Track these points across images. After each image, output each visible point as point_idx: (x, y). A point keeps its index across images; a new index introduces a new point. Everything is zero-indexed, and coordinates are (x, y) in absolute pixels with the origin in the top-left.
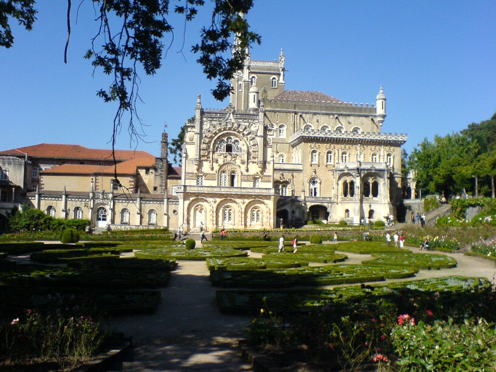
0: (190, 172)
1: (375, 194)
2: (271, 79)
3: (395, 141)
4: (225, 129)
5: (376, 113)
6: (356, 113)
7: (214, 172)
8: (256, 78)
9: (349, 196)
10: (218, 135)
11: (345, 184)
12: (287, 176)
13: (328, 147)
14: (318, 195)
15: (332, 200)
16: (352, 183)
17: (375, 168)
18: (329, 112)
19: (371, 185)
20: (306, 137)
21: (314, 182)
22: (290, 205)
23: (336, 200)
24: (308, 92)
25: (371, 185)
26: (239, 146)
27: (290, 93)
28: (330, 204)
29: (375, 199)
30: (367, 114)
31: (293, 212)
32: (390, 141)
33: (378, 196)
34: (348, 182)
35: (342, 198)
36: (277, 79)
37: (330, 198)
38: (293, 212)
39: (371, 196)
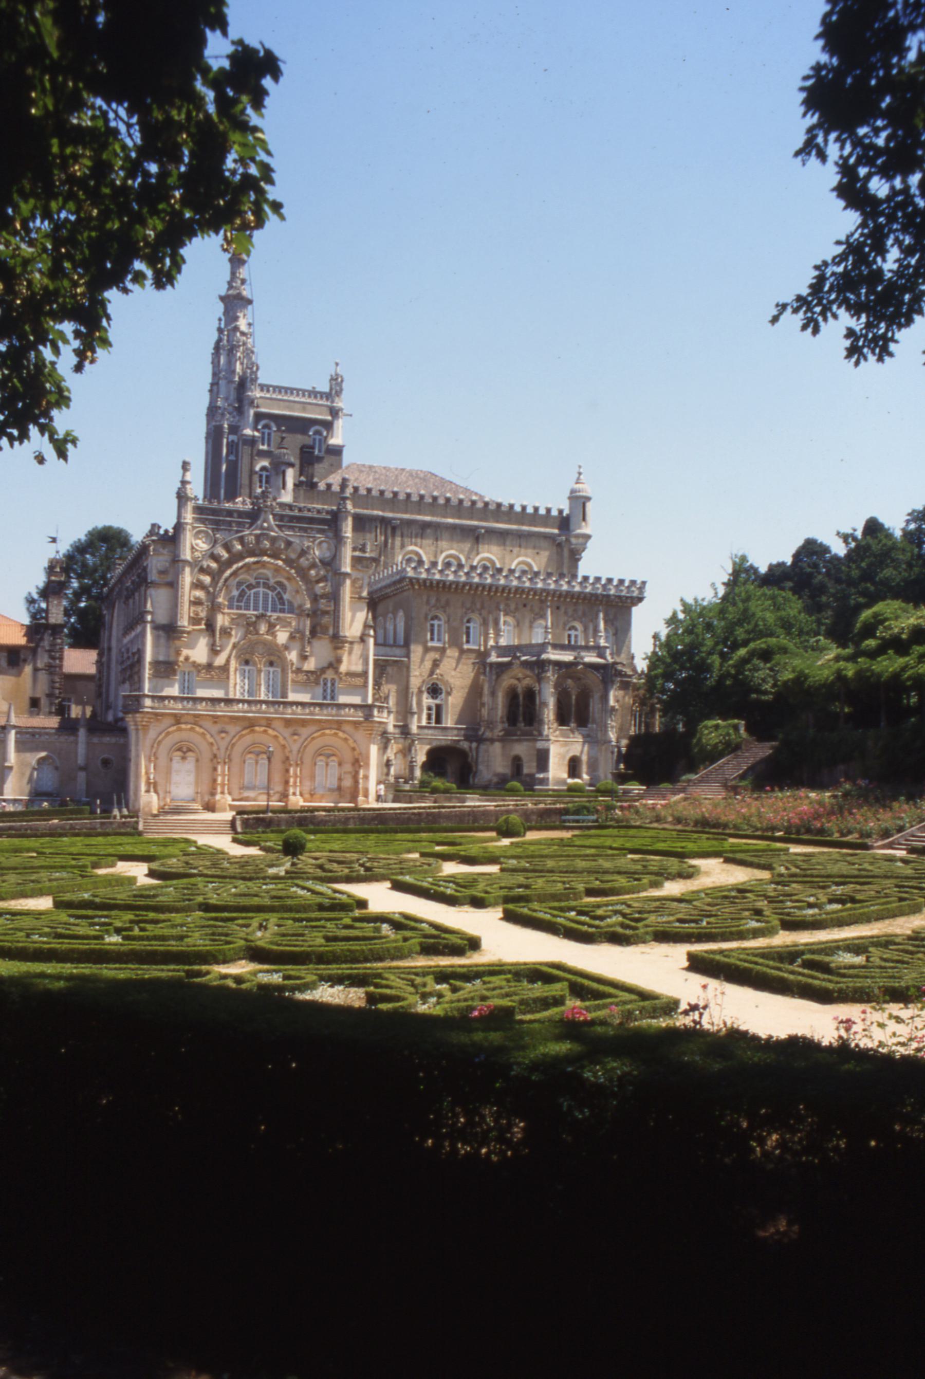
0: (161, 658)
4: (252, 554)
7: (220, 661)
9: (521, 725)
10: (235, 567)
11: (512, 695)
15: (480, 733)
16: (531, 695)
23: (488, 734)
24: (403, 470)
26: (286, 597)
27: (361, 471)
28: (474, 745)
34: (520, 690)
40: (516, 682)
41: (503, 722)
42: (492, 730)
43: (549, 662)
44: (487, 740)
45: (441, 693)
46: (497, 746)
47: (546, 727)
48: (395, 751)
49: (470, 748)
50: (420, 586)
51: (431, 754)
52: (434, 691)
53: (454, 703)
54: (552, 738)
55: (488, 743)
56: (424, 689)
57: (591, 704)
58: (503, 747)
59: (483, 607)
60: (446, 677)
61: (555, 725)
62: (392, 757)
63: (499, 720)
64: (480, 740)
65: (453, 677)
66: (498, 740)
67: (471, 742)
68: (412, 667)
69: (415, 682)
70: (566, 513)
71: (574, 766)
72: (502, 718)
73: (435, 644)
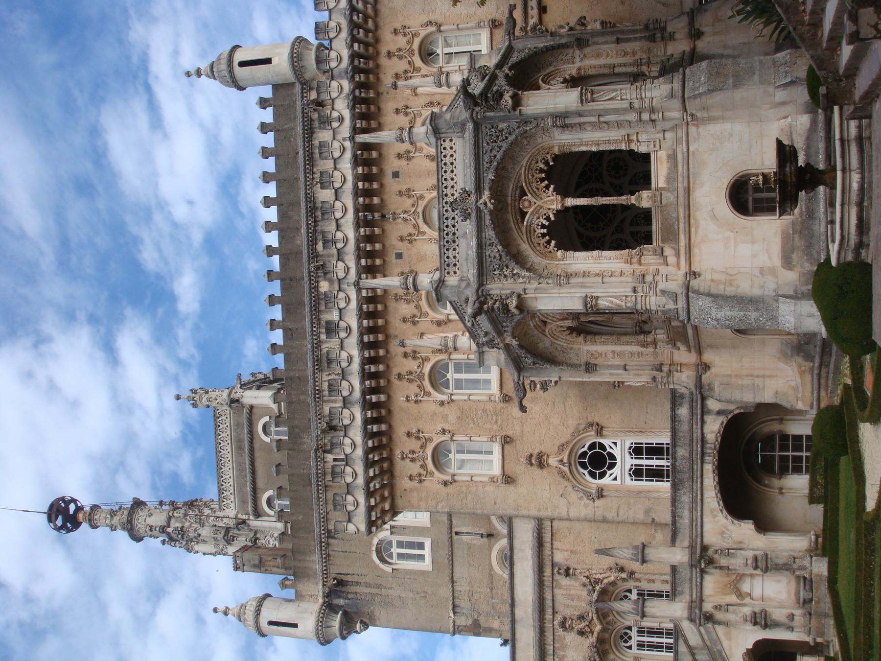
1: (632, 169)
2: (267, 440)
3: (353, 26)
5: (292, 85)
6: (302, 177)
8: (270, 493)
12: (572, 598)
13: (413, 389)
14: (665, 439)
17: (466, 193)
18: (306, 300)
19: (570, 202)
20: (370, 509)
21: (598, 461)
22: (720, 630)
25: (570, 202)
29: (660, 172)
30: (299, 130)
31: (761, 619)
32: (353, 56)
33: (643, 149)
36: (267, 419)
37: (675, 399)
38: (761, 619)
39: (644, 199)
44: (699, 379)
45: (602, 447)
48: (733, 599)
49: (719, 413)
50: (383, 499)
52: (598, 461)
55: (705, 378)
57: (584, 148)
58: (711, 346)
59: (414, 355)
64: (702, 392)
66: (700, 352)
67: (704, 411)
70: (267, 92)
72: (644, 345)
73: (496, 457)
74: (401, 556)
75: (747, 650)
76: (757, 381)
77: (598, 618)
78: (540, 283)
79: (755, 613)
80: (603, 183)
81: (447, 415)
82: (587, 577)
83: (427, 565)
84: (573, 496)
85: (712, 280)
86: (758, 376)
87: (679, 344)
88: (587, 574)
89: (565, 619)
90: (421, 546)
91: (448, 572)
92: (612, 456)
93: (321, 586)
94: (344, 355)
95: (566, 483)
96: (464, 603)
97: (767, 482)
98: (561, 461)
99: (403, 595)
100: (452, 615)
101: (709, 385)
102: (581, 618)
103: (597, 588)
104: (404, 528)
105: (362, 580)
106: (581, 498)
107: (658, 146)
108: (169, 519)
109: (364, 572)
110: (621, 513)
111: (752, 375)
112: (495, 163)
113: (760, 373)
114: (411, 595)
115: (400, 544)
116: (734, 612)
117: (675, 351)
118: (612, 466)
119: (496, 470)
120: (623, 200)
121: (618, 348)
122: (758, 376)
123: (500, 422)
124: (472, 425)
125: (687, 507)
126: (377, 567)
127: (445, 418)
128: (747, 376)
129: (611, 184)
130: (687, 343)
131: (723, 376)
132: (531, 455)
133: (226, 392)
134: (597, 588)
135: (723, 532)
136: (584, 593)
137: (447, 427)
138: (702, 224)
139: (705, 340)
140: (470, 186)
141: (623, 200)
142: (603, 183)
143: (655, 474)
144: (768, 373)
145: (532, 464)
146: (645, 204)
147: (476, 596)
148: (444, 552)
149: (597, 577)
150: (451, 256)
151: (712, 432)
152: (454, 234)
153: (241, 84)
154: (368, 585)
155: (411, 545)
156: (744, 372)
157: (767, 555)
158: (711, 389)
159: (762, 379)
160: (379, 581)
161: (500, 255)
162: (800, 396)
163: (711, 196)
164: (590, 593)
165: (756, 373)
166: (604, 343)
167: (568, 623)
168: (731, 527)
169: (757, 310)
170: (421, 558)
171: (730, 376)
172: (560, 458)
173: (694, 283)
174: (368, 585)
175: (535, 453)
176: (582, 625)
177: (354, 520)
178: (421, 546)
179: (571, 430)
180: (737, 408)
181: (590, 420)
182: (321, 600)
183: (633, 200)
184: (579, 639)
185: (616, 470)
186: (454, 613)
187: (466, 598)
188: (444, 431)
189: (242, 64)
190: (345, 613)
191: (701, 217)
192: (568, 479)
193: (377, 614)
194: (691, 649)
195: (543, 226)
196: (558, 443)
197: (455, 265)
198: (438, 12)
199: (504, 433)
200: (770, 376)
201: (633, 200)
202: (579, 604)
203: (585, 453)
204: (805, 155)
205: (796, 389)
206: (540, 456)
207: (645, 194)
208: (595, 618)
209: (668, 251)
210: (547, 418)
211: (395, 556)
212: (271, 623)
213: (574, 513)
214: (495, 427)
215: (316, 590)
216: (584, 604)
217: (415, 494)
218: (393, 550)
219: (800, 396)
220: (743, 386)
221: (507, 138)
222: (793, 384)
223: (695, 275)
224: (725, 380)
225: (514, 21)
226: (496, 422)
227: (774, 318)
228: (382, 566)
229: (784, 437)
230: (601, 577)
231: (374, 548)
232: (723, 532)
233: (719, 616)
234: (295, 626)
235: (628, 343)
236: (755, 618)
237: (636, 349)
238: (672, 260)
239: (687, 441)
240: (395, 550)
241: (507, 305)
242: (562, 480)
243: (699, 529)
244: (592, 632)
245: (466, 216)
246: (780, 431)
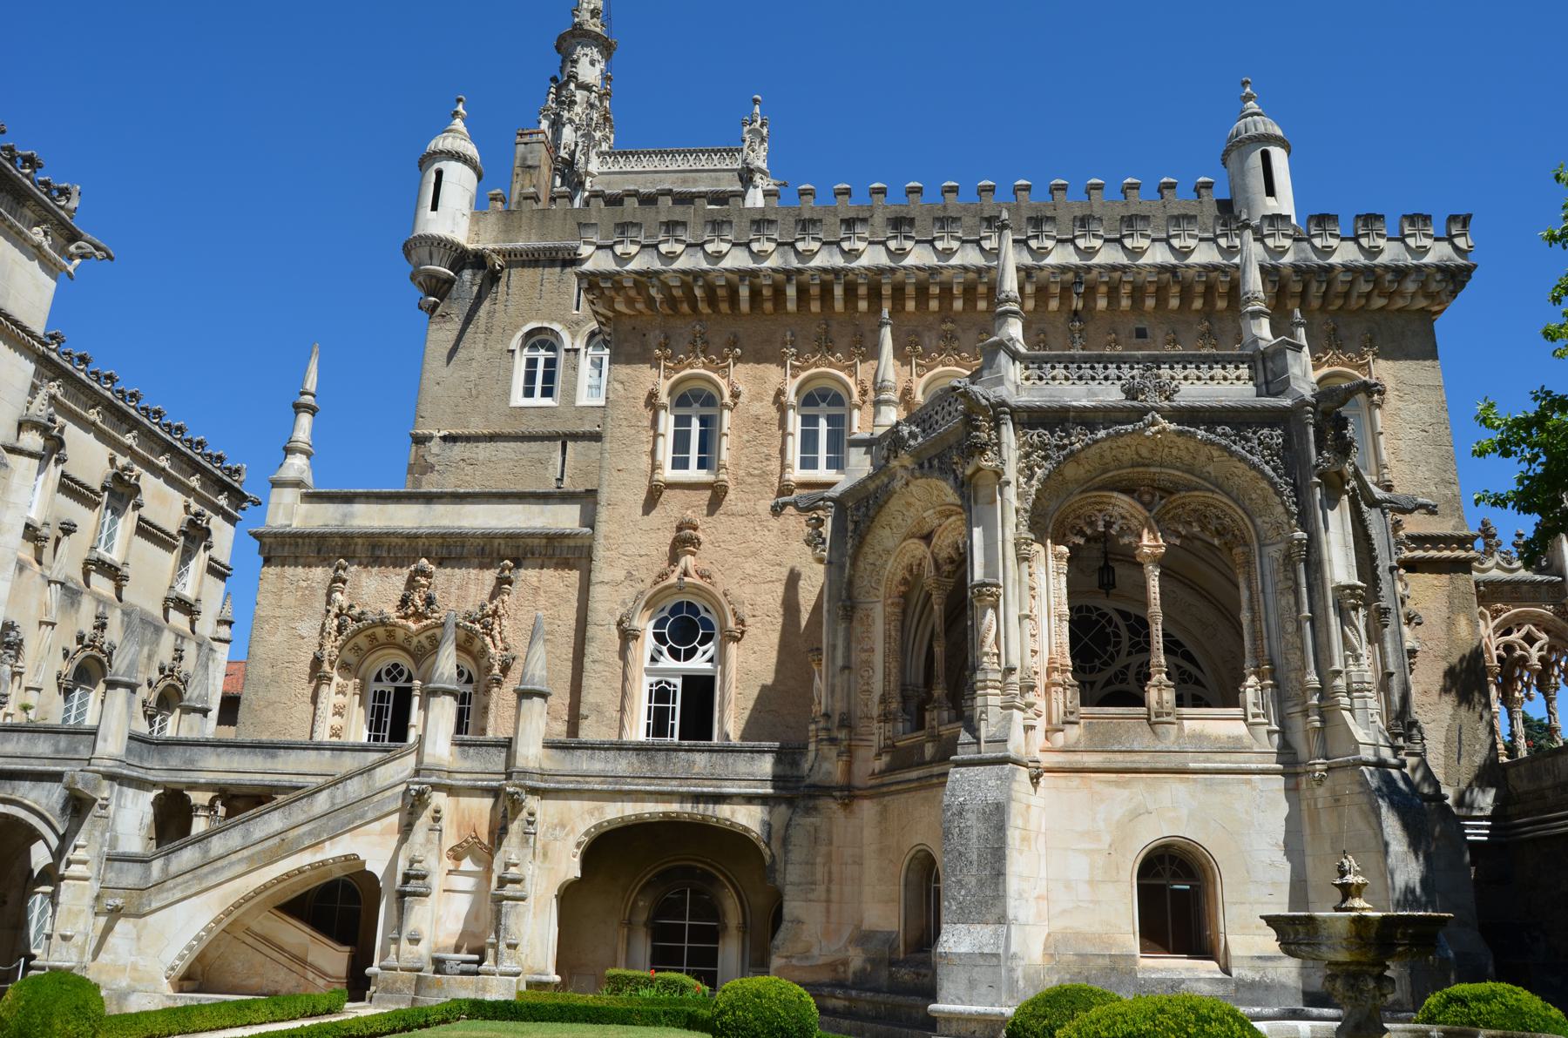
35: (889, 748)
39: (1159, 693)
40: (917, 548)
41: (886, 717)
42: (849, 753)
43: (998, 412)
44: (824, 790)
46: (867, 809)
47: (995, 700)
48: (450, 840)
50: (630, 302)
51: (603, 850)
53: (745, 670)
54: (1016, 744)
56: (645, 626)
58: (884, 813)
60: (722, 583)
61: (1064, 699)
62: (437, 866)
63: (875, 711)
65: (746, 577)
68: (600, 553)
69: (607, 605)
71: (1175, 898)
72: (884, 700)
74: (532, 363)
75: (364, 862)
76: (821, 889)
77: (426, 628)
78: (1017, 511)
79: (424, 877)
80: (1130, 653)
81: (762, 400)
82: (495, 612)
83: (518, 399)
84: (628, 593)
85: (1028, 806)
86: (828, 891)
87: (885, 759)
88: (501, 611)
89: (429, 576)
90: (547, 392)
91: (507, 430)
92: (690, 654)
93: (491, 247)
94: (861, 245)
95: (649, 581)
96: (459, 449)
97: (641, 904)
98: (686, 574)
99: (474, 364)
100: (442, 433)
101: (815, 809)
102: (429, 601)
103: (478, 627)
104: (575, 368)
105: (499, 307)
106: (624, 603)
107: (1257, 720)
108: (587, 88)
109: (511, 309)
110: (597, 667)
111: (830, 881)
112: (1224, 442)
113: (834, 896)
114: (473, 376)
115: (550, 363)
116: (428, 841)
117: (874, 751)
118: (675, 654)
119: (668, 474)
120: (1159, 658)
121: (878, 659)
122: (828, 891)
123: (750, 480)
124: (745, 437)
125: (609, 767)
126: (518, 328)
127: (757, 397)
128: (830, 872)
129: (1127, 667)
130: (890, 769)
131: (830, 833)
132: (695, 529)
133: (764, 166)
134: (478, 627)
135: (563, 826)
136: (470, 608)
137: (741, 399)
138: (1125, 793)
139: (896, 803)
140: (1180, 400)
141: (1159, 658)
142: (1130, 653)
143: (659, 724)
144: (834, 907)
145: (679, 529)
146: (1152, 695)
147: (469, 469)
148: (537, 427)
149: (496, 626)
150: (1055, 372)
151: (733, 813)
152: (1093, 378)
153: (1234, 155)
154: (491, 314)
155: (549, 377)
156: (835, 868)
157: (523, 899)
158: (809, 811)
159: (823, 896)
160: (497, 332)
161: (1064, 447)
162: (794, 962)
163: (1173, 811)
164: (468, 616)
165: (834, 888)
166: (887, 636)
167: (423, 581)
168: (572, 841)
169: (981, 884)
170: (529, 393)
171: (831, 843)
172: (692, 572)
173: (1023, 774)
174: (491, 314)
175: (700, 534)
176: (419, 603)
177: (600, 252)
178: (547, 392)
179: (735, 590)
180: (773, 856)
181: (749, 621)
182: (470, 247)
183: (1160, 677)
184: (396, 598)
185: (667, 662)
186: (445, 439)
187: (466, 455)
188: (735, 395)
189: (1266, 156)
190: (450, 282)
191: (1137, 791)
192: (656, 583)
193: (448, 326)
194: (369, 770)
195: (1108, 525)
196: (713, 569)
197: (1041, 379)
198: (1400, 404)
199: (731, 485)
200: (828, 911)
201: (1160, 677)
202: (453, 598)
203: (697, 613)
204: (1253, 981)
205: (806, 955)
206: (696, 542)
207: (1169, 696)
208: (425, 622)
209: (1074, 732)
210: (755, 554)
211: (533, 354)
212: (439, 174)
213: (597, 592)
214: (742, 473)
215: (487, 240)
216: (452, 605)
217: (638, 350)
218: (542, 352)
219: (794, 962)
220: (814, 864)
221: (1267, 463)
222: (815, 951)
223: (1035, 779)
224: (823, 835)
225: (1411, 511)
226: (750, 474)
227: (965, 917)
228: (520, 334)
229: (714, 935)
230: (495, 633)
231: (546, 325)
232: (563, 826)
233: (426, 815)
234: (435, 207)
235: (886, 675)
236: (417, 877)
237: (878, 687)
238: (1059, 739)
239: (718, 771)
240: (542, 355)
241: (983, 452)
242: (654, 576)
243: (571, 786)
244: (406, 617)
245: (1131, 393)
246: (725, 927)
